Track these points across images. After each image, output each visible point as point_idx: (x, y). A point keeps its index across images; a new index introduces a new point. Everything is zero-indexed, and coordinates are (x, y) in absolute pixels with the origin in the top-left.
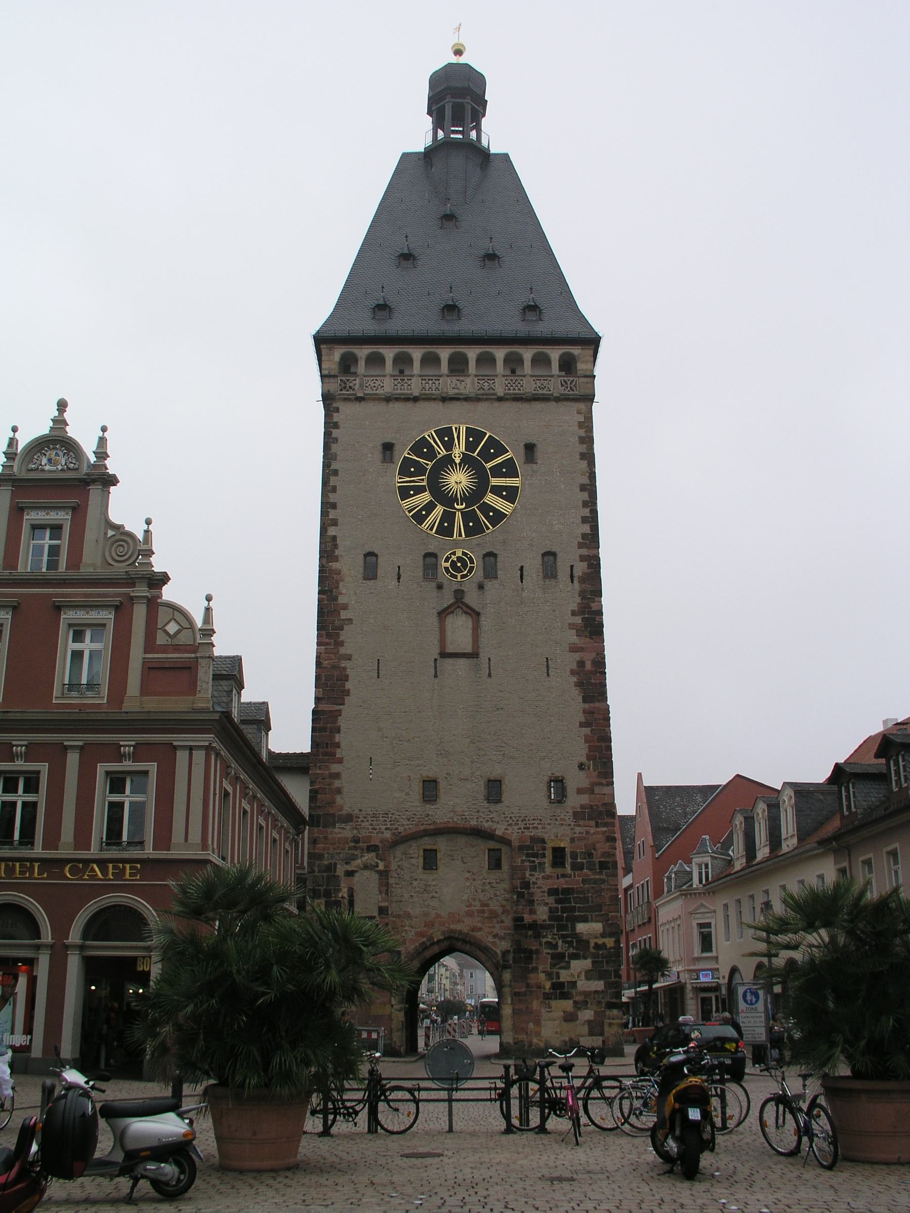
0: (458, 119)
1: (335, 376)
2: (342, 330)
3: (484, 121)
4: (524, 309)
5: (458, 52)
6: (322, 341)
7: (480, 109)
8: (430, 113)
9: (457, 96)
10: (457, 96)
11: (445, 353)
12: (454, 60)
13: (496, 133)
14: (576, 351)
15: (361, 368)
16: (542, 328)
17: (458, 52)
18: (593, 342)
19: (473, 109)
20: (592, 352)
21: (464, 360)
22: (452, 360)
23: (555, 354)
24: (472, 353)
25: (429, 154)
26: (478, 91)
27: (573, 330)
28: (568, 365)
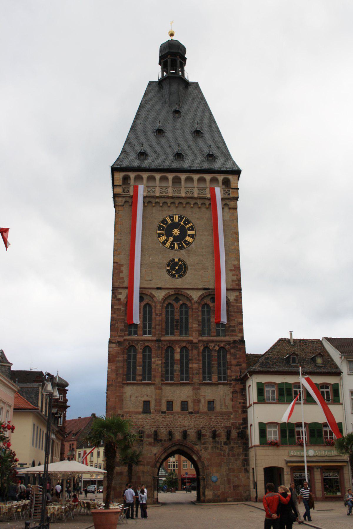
0: (174, 67)
1: (121, 186)
2: (124, 164)
3: (186, 68)
4: (207, 156)
5: (172, 35)
6: (114, 169)
7: (183, 62)
8: (160, 64)
9: (173, 56)
10: (173, 56)
11: (170, 176)
12: (170, 38)
13: (191, 73)
14: (230, 177)
15: (132, 182)
16: (215, 166)
17: (172, 35)
18: (238, 173)
19: (180, 62)
20: (237, 177)
21: (179, 179)
22: (174, 179)
23: (221, 177)
24: (183, 176)
25: (160, 82)
26: (182, 54)
27: (230, 167)
28: (226, 183)
